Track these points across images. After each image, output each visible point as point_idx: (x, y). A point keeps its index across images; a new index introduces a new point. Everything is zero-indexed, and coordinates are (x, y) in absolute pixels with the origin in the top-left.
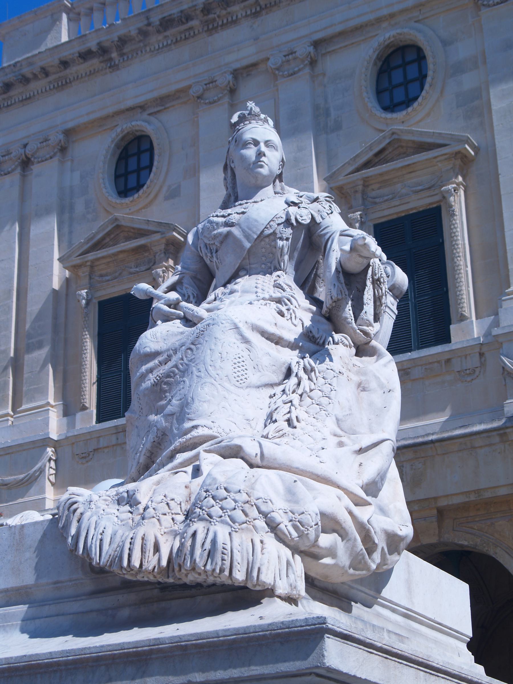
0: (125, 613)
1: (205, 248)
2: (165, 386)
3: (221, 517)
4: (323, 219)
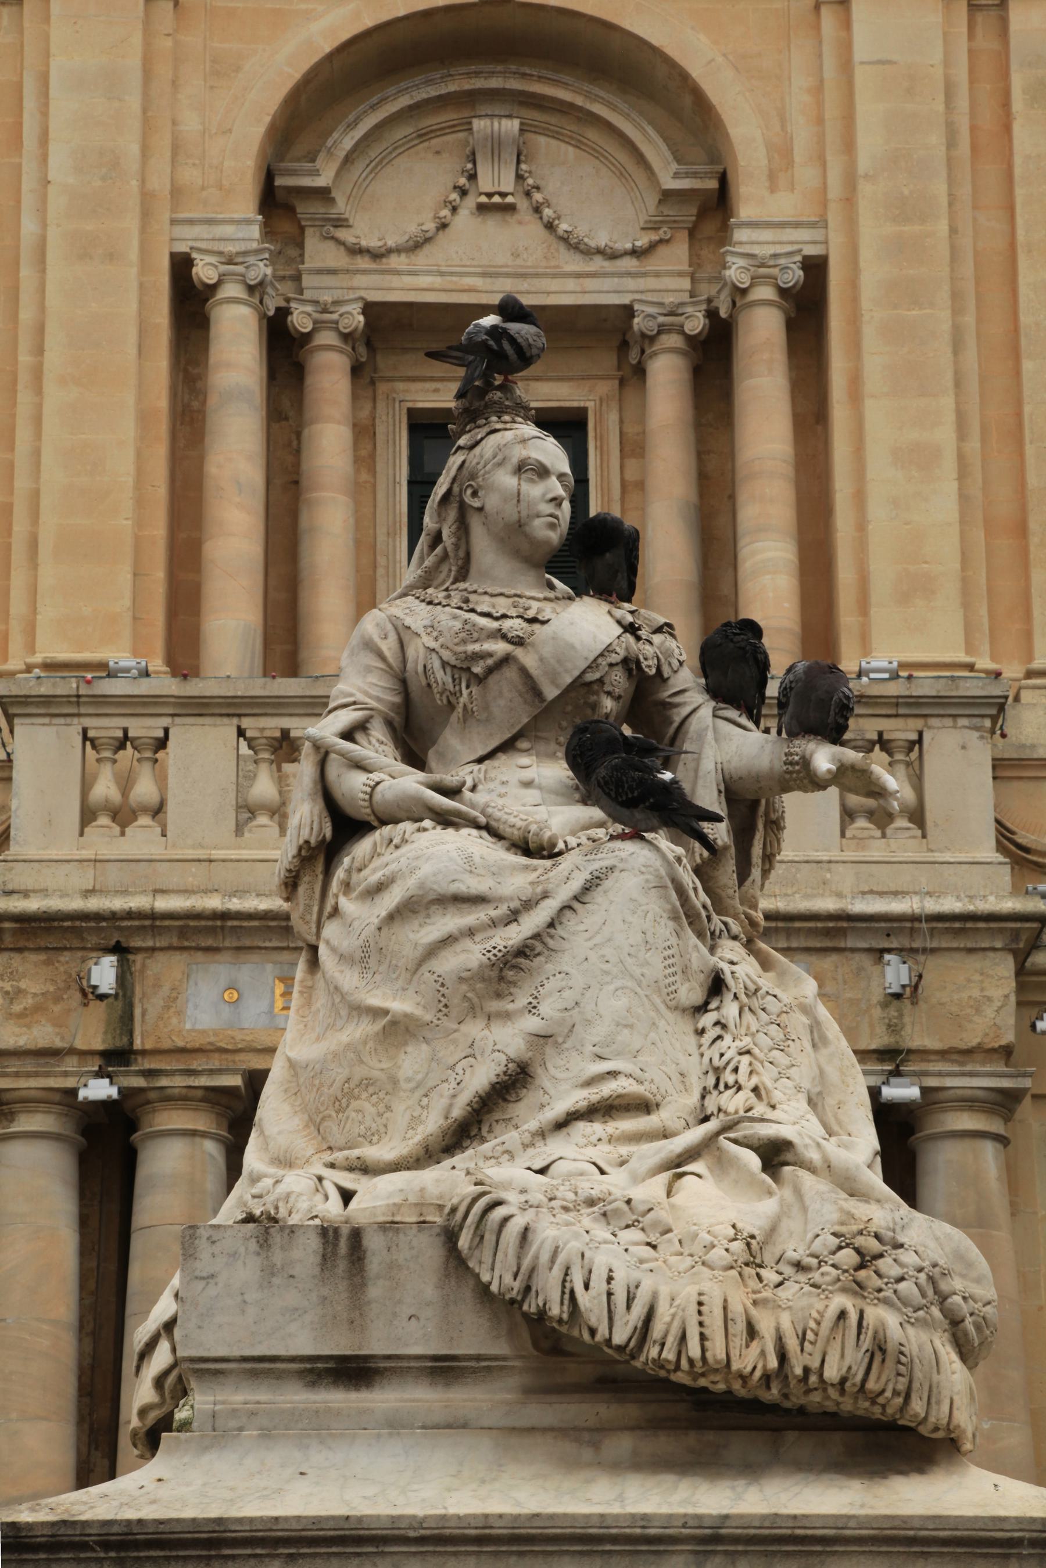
1: (442, 672)
2: (511, 973)
3: (880, 1290)
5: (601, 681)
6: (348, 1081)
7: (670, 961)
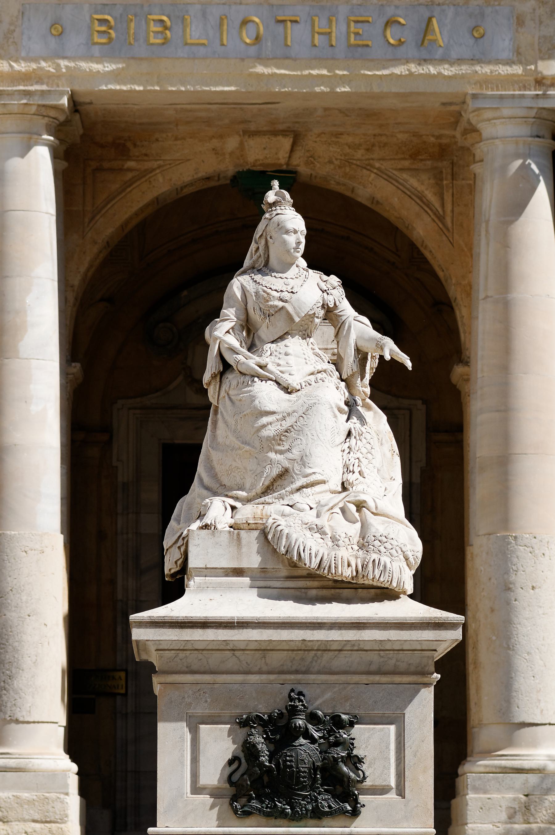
0: (313, 592)
4: (340, 303)
5: (314, 314)
6: (231, 465)
7: (333, 432)
